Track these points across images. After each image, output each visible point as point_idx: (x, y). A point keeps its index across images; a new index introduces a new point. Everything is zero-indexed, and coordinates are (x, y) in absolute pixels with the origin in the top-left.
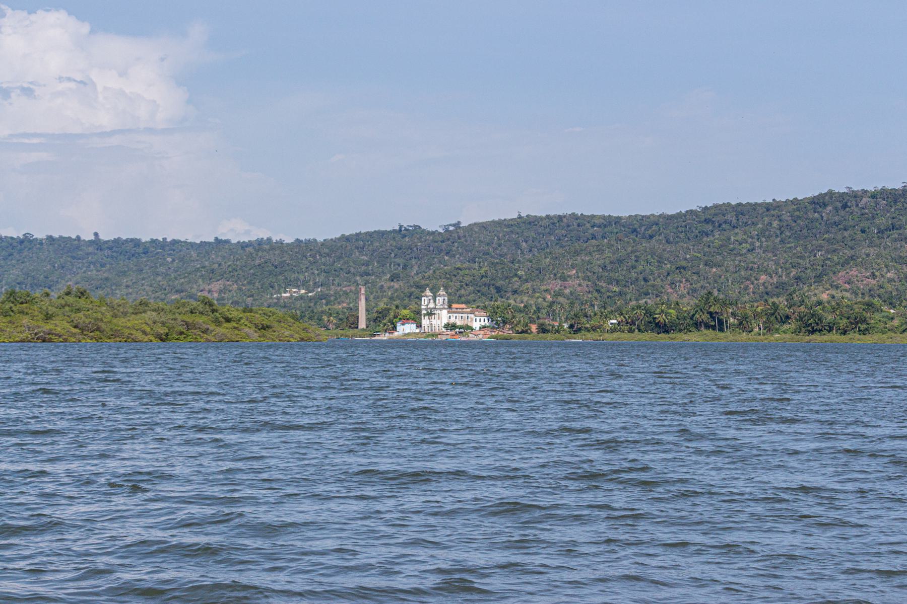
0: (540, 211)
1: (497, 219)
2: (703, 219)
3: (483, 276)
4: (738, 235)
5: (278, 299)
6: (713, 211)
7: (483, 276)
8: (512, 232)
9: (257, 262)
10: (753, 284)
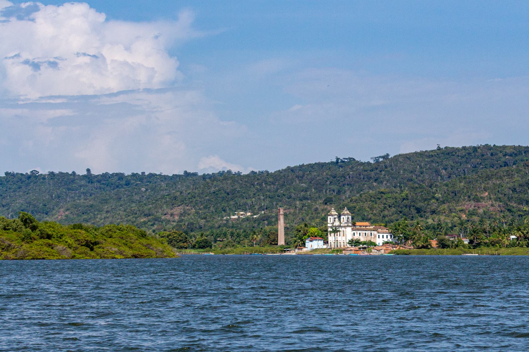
1: (419, 151)
3: (404, 199)
5: (227, 220)
7: (404, 199)
8: (432, 161)
9: (213, 190)
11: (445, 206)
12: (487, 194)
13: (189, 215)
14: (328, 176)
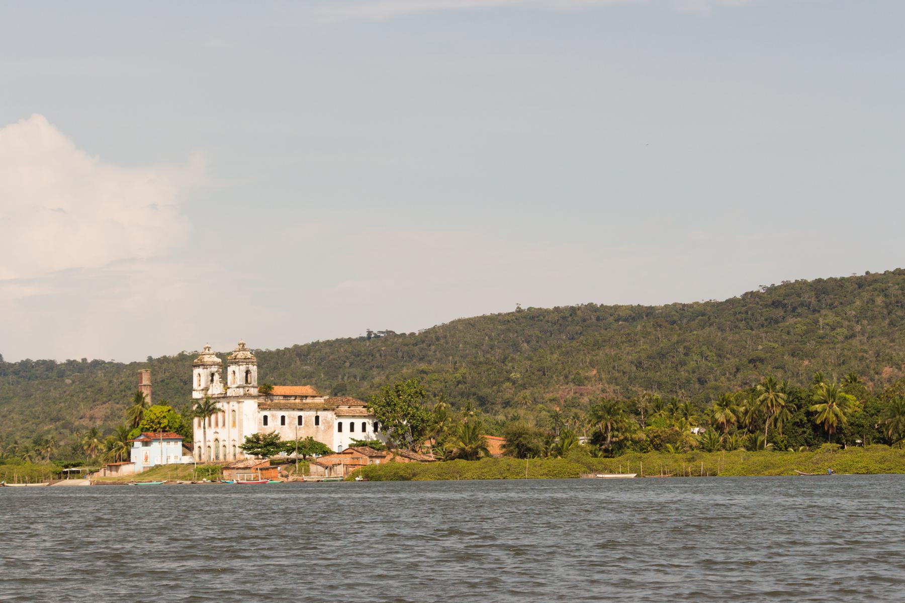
0: (547, 301)
2: (770, 302)
3: (459, 382)
4: (827, 318)
6: (782, 291)
7: (459, 382)
10: (872, 380)
11: (527, 393)
12: (595, 372)
13: (119, 417)
14: (348, 355)
